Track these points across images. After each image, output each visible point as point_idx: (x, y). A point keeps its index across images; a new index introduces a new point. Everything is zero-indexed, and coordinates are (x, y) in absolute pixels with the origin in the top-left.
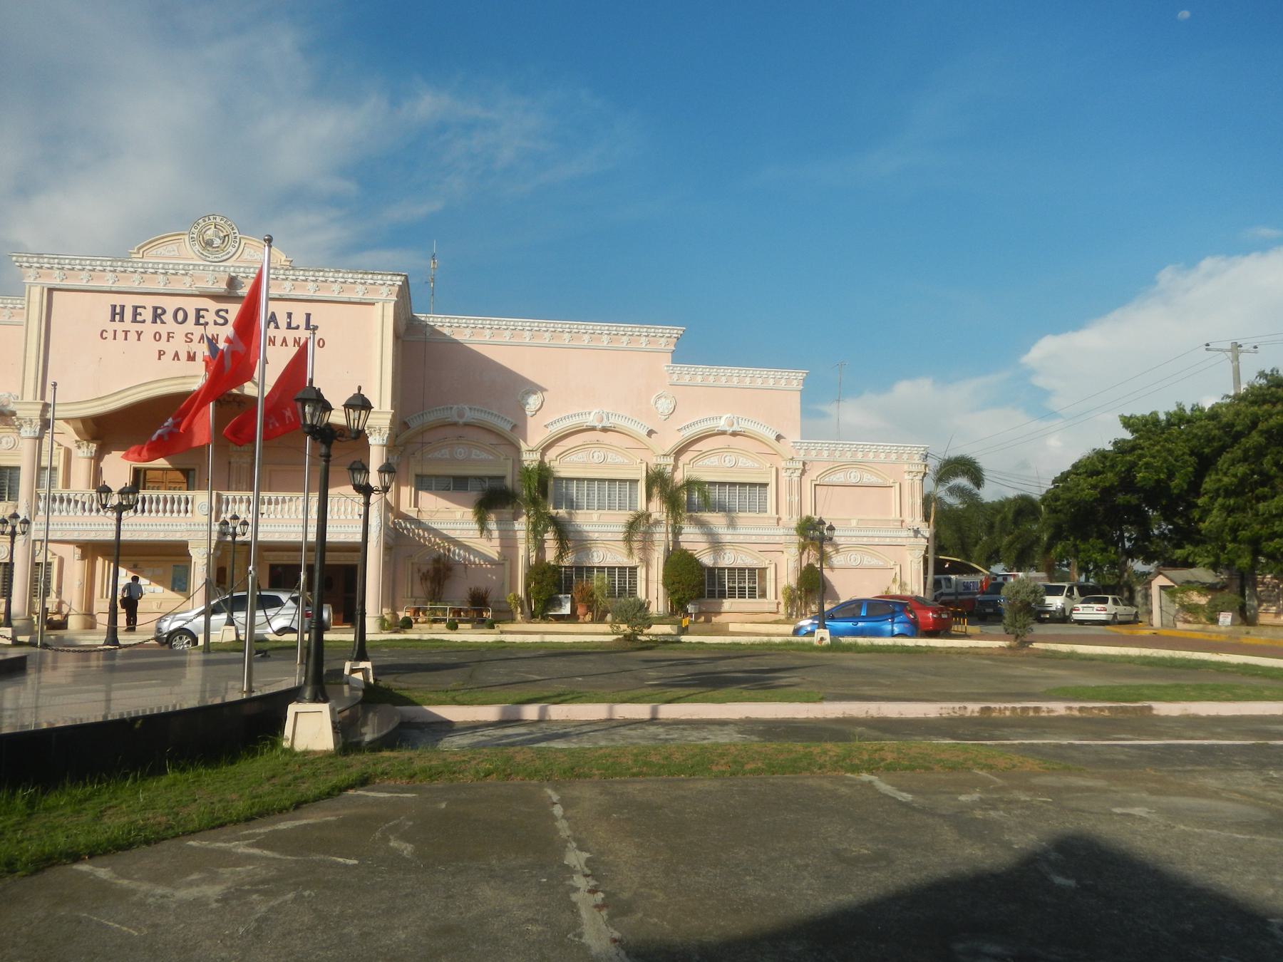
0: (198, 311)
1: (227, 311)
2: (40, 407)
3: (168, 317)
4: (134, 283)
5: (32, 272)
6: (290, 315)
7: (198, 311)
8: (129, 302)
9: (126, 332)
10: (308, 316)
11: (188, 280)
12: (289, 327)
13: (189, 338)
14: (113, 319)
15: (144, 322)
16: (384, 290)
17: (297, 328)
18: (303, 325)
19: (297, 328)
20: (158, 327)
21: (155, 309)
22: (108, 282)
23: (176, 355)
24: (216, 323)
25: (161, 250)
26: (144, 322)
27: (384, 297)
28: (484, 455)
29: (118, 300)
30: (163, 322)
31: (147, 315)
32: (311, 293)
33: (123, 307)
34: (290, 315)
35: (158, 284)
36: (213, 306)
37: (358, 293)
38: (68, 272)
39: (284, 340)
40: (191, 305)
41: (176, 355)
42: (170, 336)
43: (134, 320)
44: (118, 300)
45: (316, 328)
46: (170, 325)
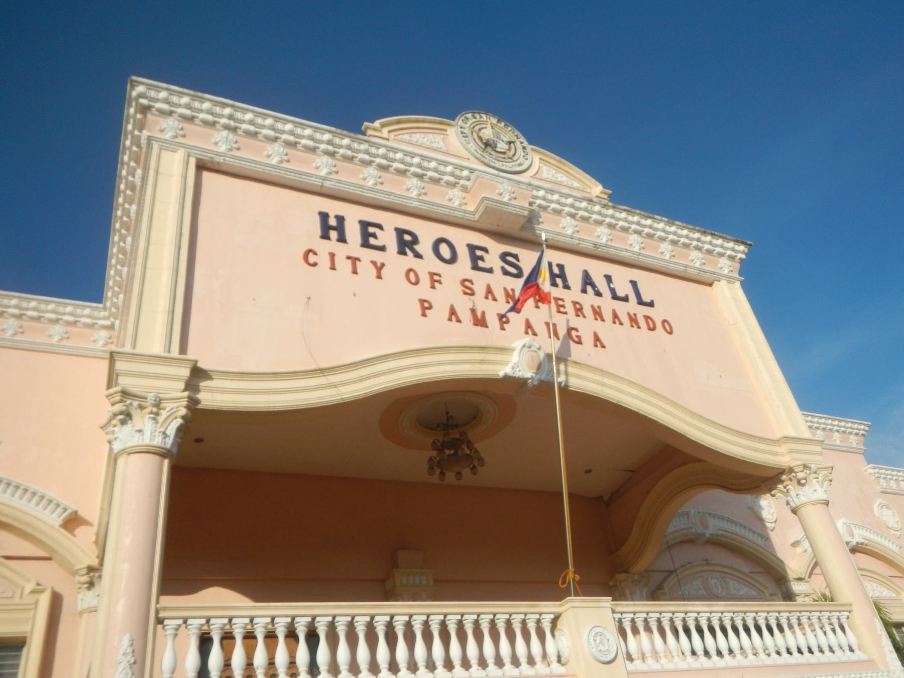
0: (472, 248)
1: (516, 257)
2: (186, 372)
3: (425, 247)
4: (367, 179)
5: (171, 123)
6: (609, 279)
7: (472, 248)
8: (353, 215)
9: (354, 260)
10: (634, 284)
11: (456, 192)
12: (615, 297)
13: (468, 289)
14: (325, 236)
15: (382, 249)
16: (724, 262)
17: (626, 299)
18: (633, 298)
19: (626, 299)
20: (409, 260)
21: (400, 232)
22: (320, 168)
23: (453, 312)
24: (506, 273)
25: (417, 137)
26: (382, 249)
27: (726, 272)
28: (745, 590)
29: (334, 208)
30: (418, 256)
31: (387, 238)
32: (636, 249)
33: (340, 219)
34: (609, 279)
35: (409, 190)
36: (496, 248)
37: (695, 260)
38: (245, 141)
39: (615, 316)
40: (462, 239)
41: (453, 312)
42: (435, 279)
43: (365, 244)
44: (334, 208)
45: (651, 304)
46: (430, 263)
